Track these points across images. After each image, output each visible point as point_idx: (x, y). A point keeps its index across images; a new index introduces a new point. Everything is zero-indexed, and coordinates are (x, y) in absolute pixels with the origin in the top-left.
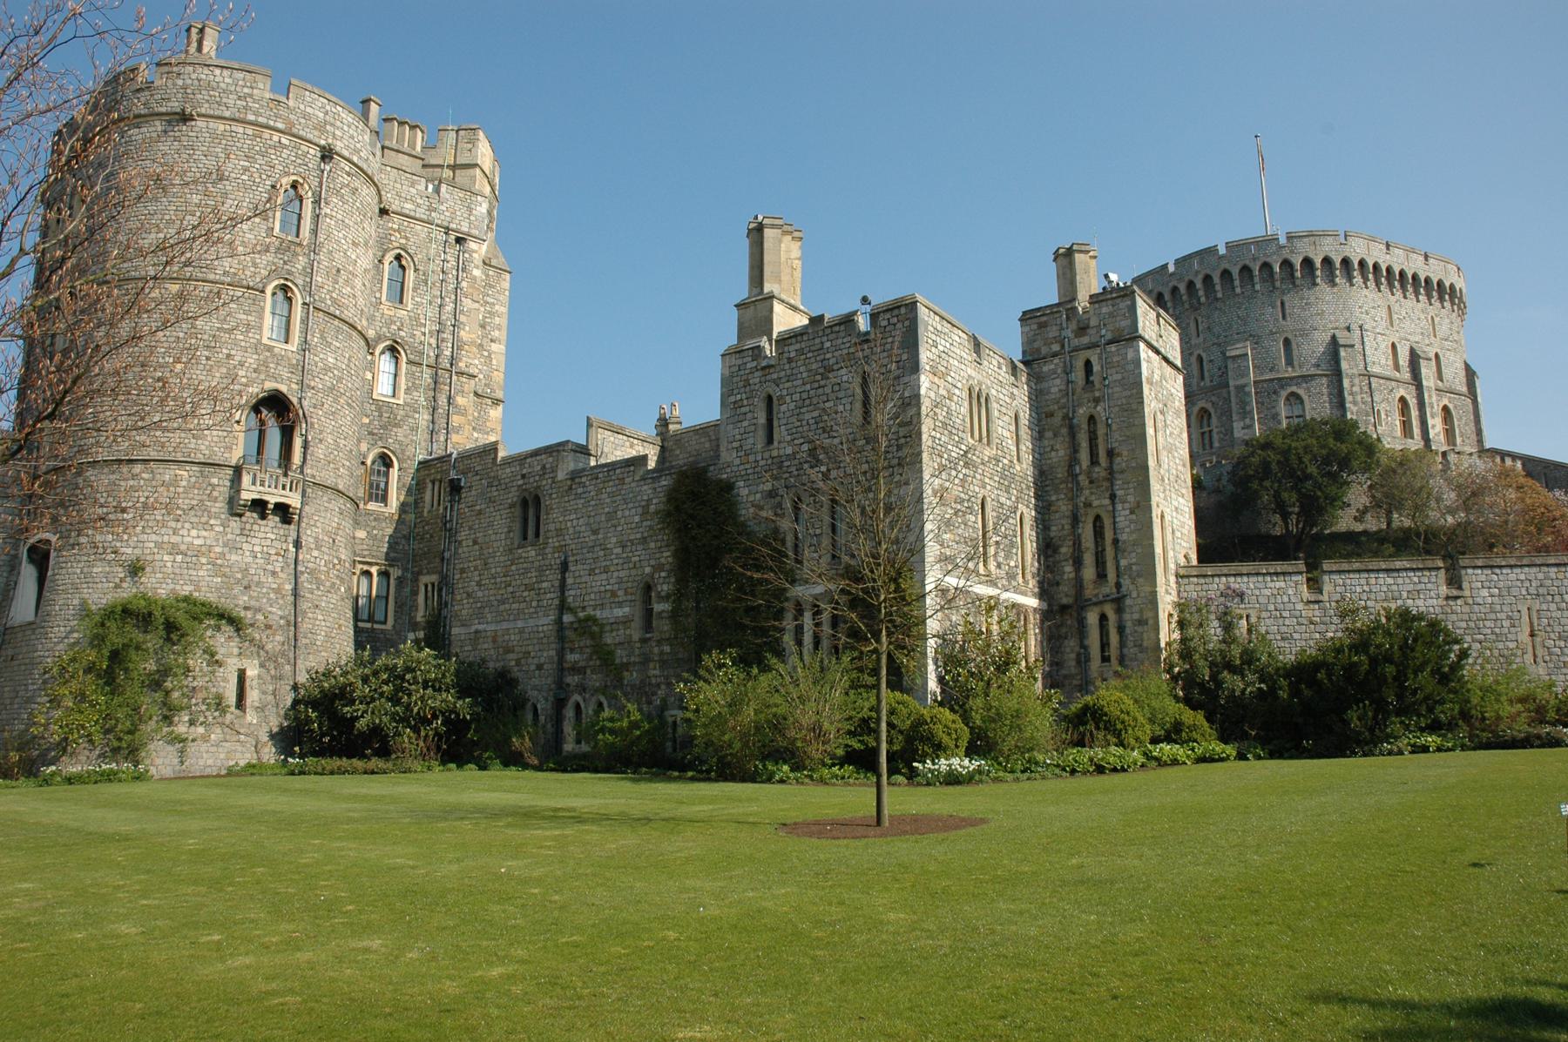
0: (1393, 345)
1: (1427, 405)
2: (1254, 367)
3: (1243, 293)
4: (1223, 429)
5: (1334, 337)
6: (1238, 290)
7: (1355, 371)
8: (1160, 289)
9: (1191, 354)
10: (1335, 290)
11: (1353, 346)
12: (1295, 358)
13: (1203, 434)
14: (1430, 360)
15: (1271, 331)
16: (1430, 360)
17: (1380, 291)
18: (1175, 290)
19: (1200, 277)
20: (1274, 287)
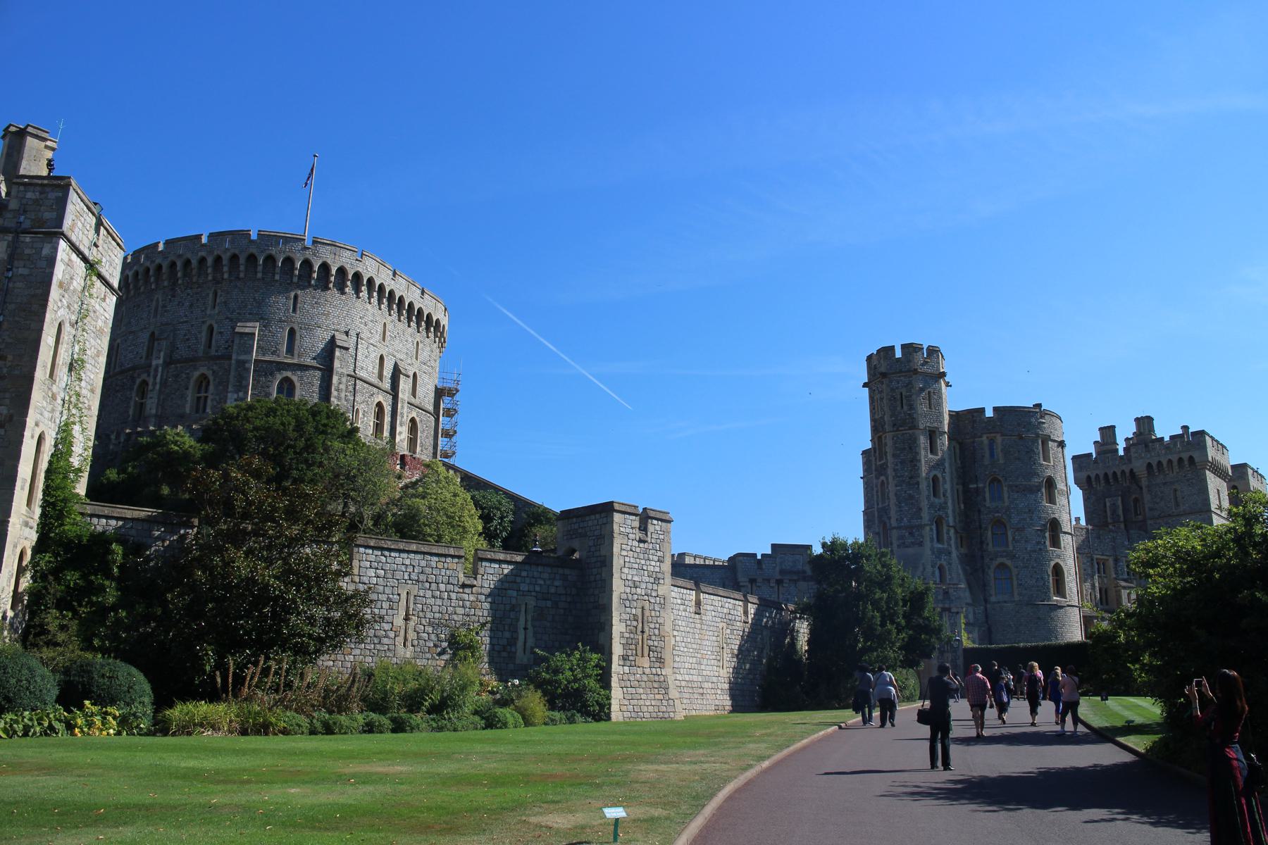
0: (382, 358)
1: (399, 414)
2: (258, 348)
3: (263, 279)
4: (217, 398)
5: (333, 337)
6: (259, 275)
7: (344, 371)
8: (189, 255)
9: (203, 322)
10: (343, 297)
11: (347, 349)
12: (296, 347)
13: (199, 398)
14: (408, 377)
16: (408, 377)
17: (380, 309)
18: (202, 261)
19: (229, 254)
20: (292, 281)
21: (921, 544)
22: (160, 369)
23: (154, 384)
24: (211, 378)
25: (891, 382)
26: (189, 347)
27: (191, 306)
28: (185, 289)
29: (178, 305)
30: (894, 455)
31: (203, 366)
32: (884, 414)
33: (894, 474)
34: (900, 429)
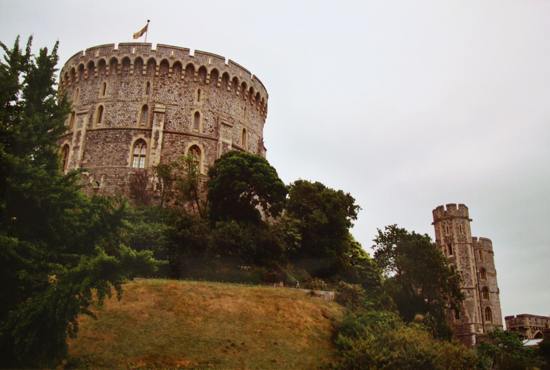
8: (180, 60)
9: (191, 109)
15: (240, 121)
21: (473, 297)
22: (161, 135)
23: (156, 144)
24: (202, 151)
25: (456, 220)
26: (180, 123)
27: (180, 95)
28: (174, 82)
29: (169, 91)
30: (459, 254)
31: (196, 140)
32: (453, 234)
33: (459, 263)
34: (462, 242)
